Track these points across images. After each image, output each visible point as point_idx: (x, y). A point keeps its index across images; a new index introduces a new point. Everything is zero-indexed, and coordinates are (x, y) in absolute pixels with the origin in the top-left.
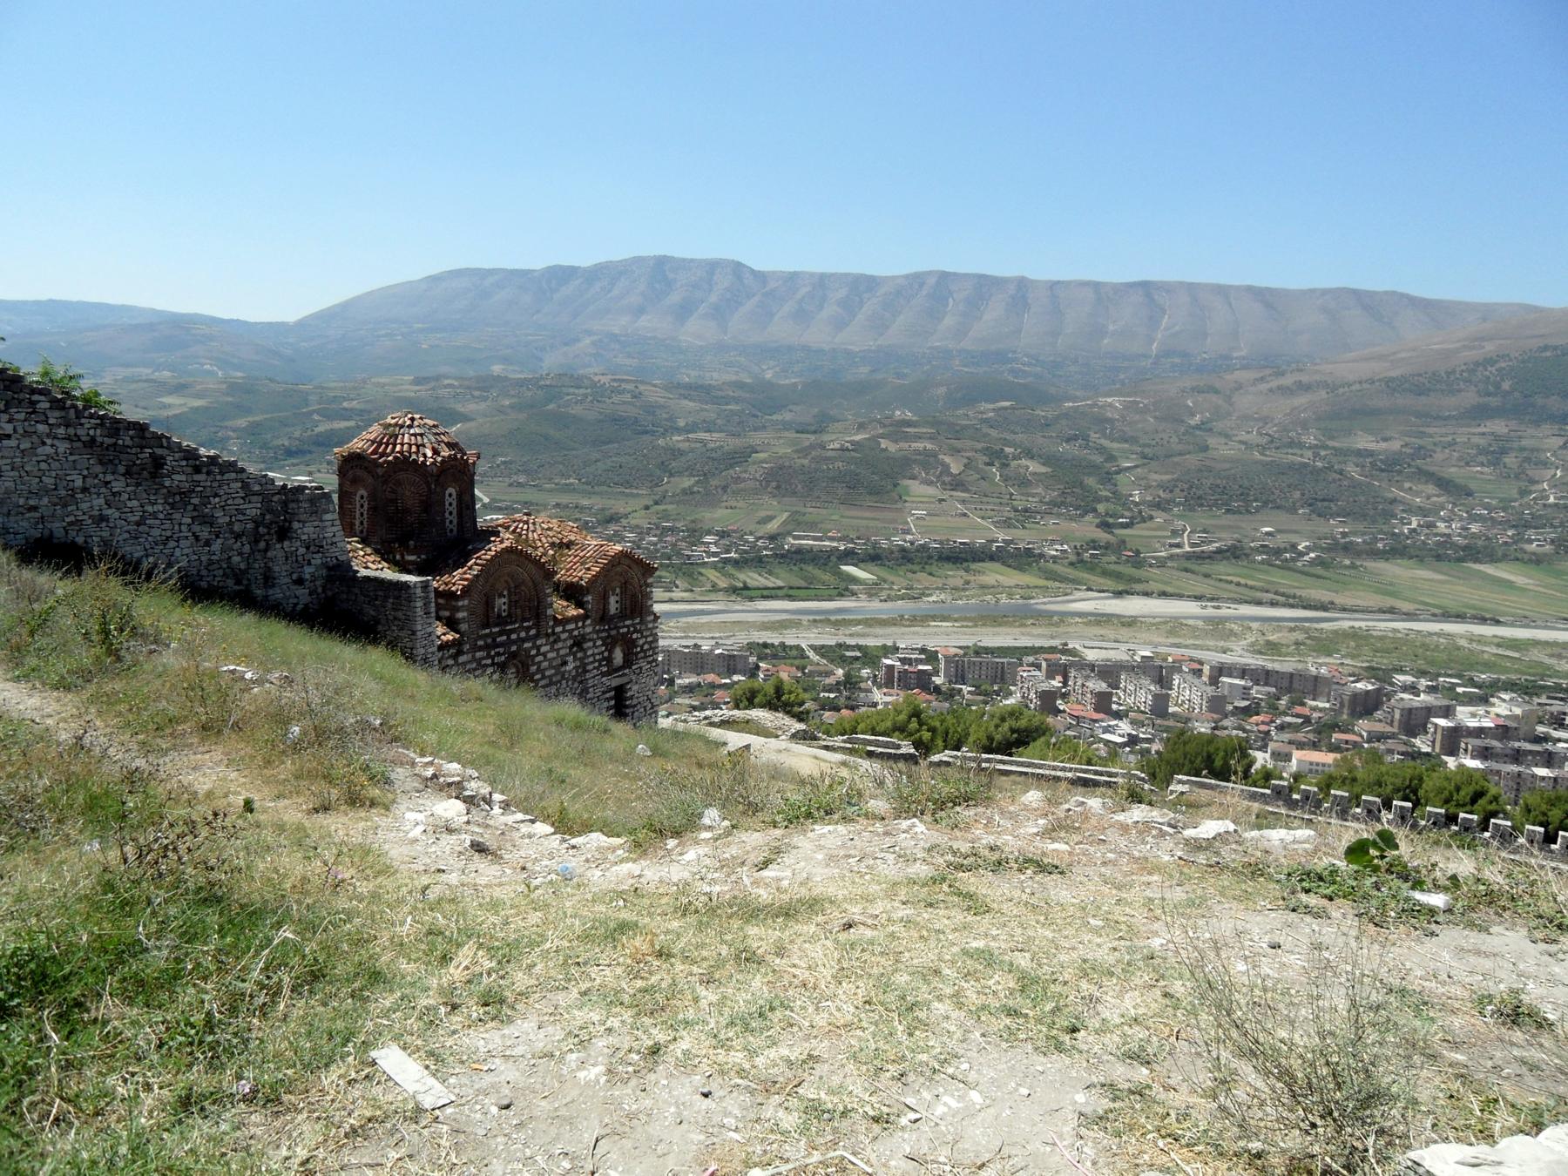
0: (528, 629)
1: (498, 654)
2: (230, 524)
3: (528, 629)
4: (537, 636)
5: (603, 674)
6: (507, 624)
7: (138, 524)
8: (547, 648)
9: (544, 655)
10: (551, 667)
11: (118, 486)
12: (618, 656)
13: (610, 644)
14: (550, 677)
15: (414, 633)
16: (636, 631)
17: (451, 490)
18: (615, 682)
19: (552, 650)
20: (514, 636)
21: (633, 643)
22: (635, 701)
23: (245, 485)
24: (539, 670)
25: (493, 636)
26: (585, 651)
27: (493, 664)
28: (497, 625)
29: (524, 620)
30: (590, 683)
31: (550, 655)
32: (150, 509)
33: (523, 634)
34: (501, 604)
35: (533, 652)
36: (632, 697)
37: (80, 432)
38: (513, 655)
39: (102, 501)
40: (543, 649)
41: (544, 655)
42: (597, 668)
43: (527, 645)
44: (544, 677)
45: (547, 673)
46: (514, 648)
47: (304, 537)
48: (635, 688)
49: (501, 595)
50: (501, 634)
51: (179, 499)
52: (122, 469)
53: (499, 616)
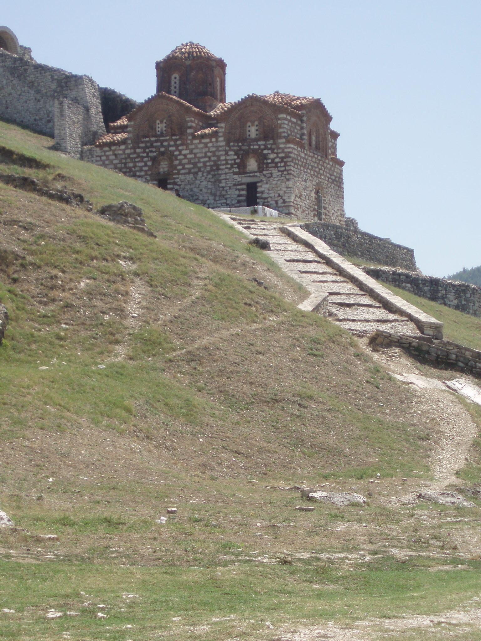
0: (177, 140)
1: (151, 151)
2: (46, 93)
3: (177, 140)
4: (181, 145)
5: (235, 173)
6: (163, 136)
7: (20, 95)
8: (188, 152)
9: (185, 155)
10: (190, 163)
11: (14, 82)
12: (252, 164)
13: (243, 156)
14: (190, 169)
15: (54, 122)
16: (266, 148)
18: (246, 180)
19: (191, 153)
20: (165, 144)
21: (265, 157)
22: (265, 195)
23: (52, 77)
24: (180, 164)
25: (152, 143)
26: (218, 157)
27: (147, 156)
28: (153, 137)
30: (223, 177)
31: (189, 156)
32: (23, 89)
33: (172, 143)
36: (262, 192)
37: (6, 64)
38: (163, 154)
39: (10, 88)
40: (184, 152)
42: (230, 169)
43: (171, 149)
44: (184, 168)
45: (187, 166)
46: (162, 149)
47: (72, 96)
48: (267, 186)
49: (161, 122)
50: (156, 141)
51: (31, 85)
52: (16, 75)
53: (162, 133)
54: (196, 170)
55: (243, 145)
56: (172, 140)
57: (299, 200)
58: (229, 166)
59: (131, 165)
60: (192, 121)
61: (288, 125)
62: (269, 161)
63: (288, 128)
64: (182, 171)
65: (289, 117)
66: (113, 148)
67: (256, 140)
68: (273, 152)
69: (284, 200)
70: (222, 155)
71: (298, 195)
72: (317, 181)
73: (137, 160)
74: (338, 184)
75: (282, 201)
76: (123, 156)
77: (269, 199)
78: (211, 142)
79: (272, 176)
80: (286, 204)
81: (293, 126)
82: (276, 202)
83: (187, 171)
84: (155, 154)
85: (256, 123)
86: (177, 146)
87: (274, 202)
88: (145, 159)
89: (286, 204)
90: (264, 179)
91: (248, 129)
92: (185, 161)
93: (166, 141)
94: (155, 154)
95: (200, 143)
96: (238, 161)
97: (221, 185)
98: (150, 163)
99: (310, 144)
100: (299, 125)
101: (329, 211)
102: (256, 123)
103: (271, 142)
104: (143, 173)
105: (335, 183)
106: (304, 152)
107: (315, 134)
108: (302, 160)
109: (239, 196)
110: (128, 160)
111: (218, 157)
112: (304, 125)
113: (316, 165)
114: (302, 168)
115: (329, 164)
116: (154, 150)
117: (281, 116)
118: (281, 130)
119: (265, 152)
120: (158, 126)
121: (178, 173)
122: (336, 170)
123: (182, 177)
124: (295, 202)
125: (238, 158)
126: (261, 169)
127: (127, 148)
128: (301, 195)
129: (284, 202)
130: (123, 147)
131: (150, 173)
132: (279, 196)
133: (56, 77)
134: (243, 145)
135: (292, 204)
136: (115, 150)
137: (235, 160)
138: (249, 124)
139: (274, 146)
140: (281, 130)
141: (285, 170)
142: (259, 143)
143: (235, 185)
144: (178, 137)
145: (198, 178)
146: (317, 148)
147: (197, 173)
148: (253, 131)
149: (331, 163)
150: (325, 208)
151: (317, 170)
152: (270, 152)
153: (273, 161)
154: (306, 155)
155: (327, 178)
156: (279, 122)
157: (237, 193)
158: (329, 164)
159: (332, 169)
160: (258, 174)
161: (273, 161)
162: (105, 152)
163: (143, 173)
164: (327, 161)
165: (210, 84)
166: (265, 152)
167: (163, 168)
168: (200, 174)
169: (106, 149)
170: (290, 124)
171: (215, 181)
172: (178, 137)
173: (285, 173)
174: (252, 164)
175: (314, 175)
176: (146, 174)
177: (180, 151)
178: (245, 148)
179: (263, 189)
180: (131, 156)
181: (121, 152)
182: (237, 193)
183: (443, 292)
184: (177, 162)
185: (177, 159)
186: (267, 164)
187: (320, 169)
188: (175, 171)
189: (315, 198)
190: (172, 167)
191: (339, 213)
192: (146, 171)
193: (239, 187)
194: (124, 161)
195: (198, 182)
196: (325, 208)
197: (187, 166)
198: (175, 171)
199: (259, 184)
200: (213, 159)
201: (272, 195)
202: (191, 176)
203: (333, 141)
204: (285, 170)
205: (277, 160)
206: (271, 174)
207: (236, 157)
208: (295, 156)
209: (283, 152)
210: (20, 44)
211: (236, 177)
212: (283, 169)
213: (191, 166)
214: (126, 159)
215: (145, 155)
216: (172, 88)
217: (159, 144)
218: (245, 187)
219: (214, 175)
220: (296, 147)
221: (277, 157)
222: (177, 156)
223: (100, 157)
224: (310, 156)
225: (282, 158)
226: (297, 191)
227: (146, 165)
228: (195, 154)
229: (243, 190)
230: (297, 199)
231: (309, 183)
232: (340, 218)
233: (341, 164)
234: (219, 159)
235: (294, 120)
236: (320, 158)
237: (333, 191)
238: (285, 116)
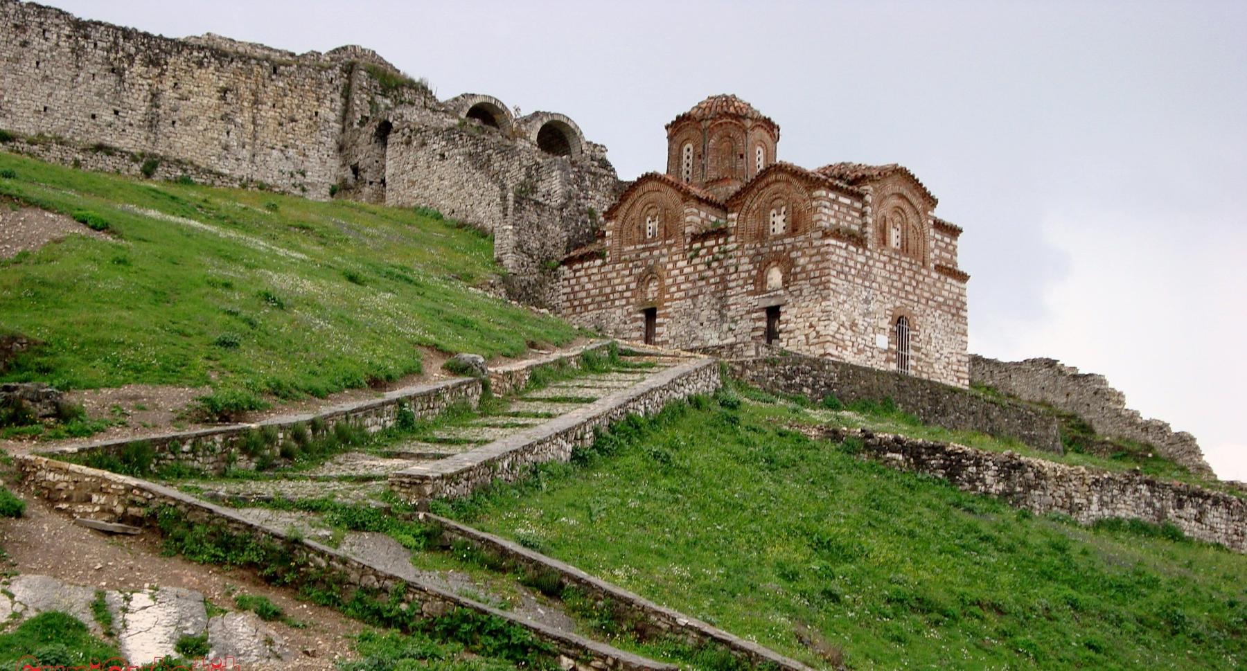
0: (670, 246)
1: (636, 267)
3: (670, 246)
5: (749, 293)
9: (681, 270)
10: (687, 280)
12: (775, 277)
16: (794, 248)
17: (689, 145)
20: (656, 253)
21: (792, 262)
22: (791, 326)
26: (726, 268)
27: (630, 274)
28: (639, 243)
29: (666, 238)
30: (731, 300)
31: (686, 270)
34: (652, 226)
35: (670, 266)
36: (787, 322)
38: (650, 270)
40: (680, 264)
41: (681, 270)
44: (679, 290)
45: (683, 287)
46: (651, 262)
48: (795, 311)
50: (644, 250)
54: (696, 292)
55: (762, 246)
56: (665, 245)
57: (850, 333)
58: (741, 282)
59: (608, 290)
60: (692, 214)
61: (831, 208)
62: (798, 269)
63: (832, 213)
64: (677, 295)
65: (832, 196)
66: (586, 264)
67: (782, 237)
68: (804, 255)
69: (818, 332)
70: (732, 265)
71: (847, 324)
72: (898, 304)
73: (618, 281)
74: (954, 311)
75: (814, 334)
76: (598, 277)
77: (797, 333)
78: (717, 244)
79: (801, 294)
80: (821, 339)
81: (845, 210)
82: (807, 336)
83: (682, 294)
84: (641, 270)
85: (783, 209)
86: (671, 255)
87: (803, 337)
88: (627, 280)
89: (821, 339)
90: (790, 300)
91: (772, 219)
92: (681, 279)
93: (656, 248)
94: (641, 270)
95: (703, 247)
96: (754, 273)
97: (729, 314)
98: (633, 286)
99: (883, 241)
100: (855, 210)
101: (926, 355)
102: (783, 209)
103: (802, 238)
104: (624, 302)
105: (946, 308)
106: (863, 253)
107: (899, 226)
108: (859, 266)
109: (754, 329)
110: (606, 282)
111: (726, 268)
112: (869, 209)
113: (895, 277)
114: (860, 281)
115: (929, 276)
116: (639, 263)
117: (817, 193)
118: (816, 217)
119: (793, 255)
120: (648, 225)
121: (672, 299)
122: (947, 287)
123: (676, 304)
124: (838, 336)
125: (755, 268)
126: (786, 282)
127: (604, 264)
128: (854, 324)
129: (818, 335)
130: (599, 262)
131: (633, 300)
132: (811, 326)
133: (525, 163)
134: (762, 246)
135: (830, 338)
136: (589, 267)
137: (749, 271)
138: (774, 211)
139: (806, 244)
140: (816, 217)
141: (820, 284)
142: (787, 241)
143: (748, 312)
144: (672, 241)
145: (699, 305)
146: (904, 249)
147: (696, 296)
148: (778, 223)
149: (935, 275)
150: (918, 349)
151: (899, 285)
152: (799, 253)
153: (804, 267)
154: (867, 258)
155: (924, 301)
156: (814, 204)
157: (751, 324)
158: (929, 276)
159: (939, 285)
160: (781, 292)
161: (804, 267)
162: (575, 271)
163: (624, 302)
164: (924, 272)
165: (742, 156)
166: (793, 255)
167: (653, 292)
168: (701, 297)
169: (578, 266)
170: (836, 207)
171: (723, 307)
172: (672, 241)
173: (821, 287)
174: (775, 277)
175: (890, 292)
176: (628, 304)
177: (675, 263)
178: (763, 250)
179: (788, 317)
180: (609, 276)
181: (595, 270)
182: (751, 324)
183: (972, 469)
184: (670, 281)
185: (669, 277)
186: (796, 274)
187: (904, 284)
188: (667, 296)
189: (891, 330)
190: (663, 290)
191: (954, 359)
192: (627, 298)
193: (754, 315)
194: (599, 284)
195: (697, 311)
196: (918, 349)
197: (683, 287)
198: (667, 296)
199: (782, 309)
200: (719, 271)
201: (800, 326)
202: (689, 302)
203: (947, 240)
204: (820, 284)
205: (810, 267)
206: (801, 291)
207: (751, 267)
208: (841, 260)
209: (818, 253)
210: (588, 139)
211: (750, 298)
212: (817, 281)
213: (690, 285)
214: (601, 280)
215: (627, 272)
216: (684, 166)
217: (647, 253)
218: (764, 314)
219: (721, 298)
220: (844, 245)
221: (810, 262)
222: (670, 270)
223: (569, 280)
224: (879, 261)
225: (817, 263)
226: (843, 318)
227: (628, 289)
228: (695, 266)
229: (760, 319)
230: (842, 330)
231: (872, 307)
232: (955, 367)
233: (963, 277)
234: (727, 273)
235: (847, 201)
236: (906, 265)
237: (939, 322)
238: (824, 193)
